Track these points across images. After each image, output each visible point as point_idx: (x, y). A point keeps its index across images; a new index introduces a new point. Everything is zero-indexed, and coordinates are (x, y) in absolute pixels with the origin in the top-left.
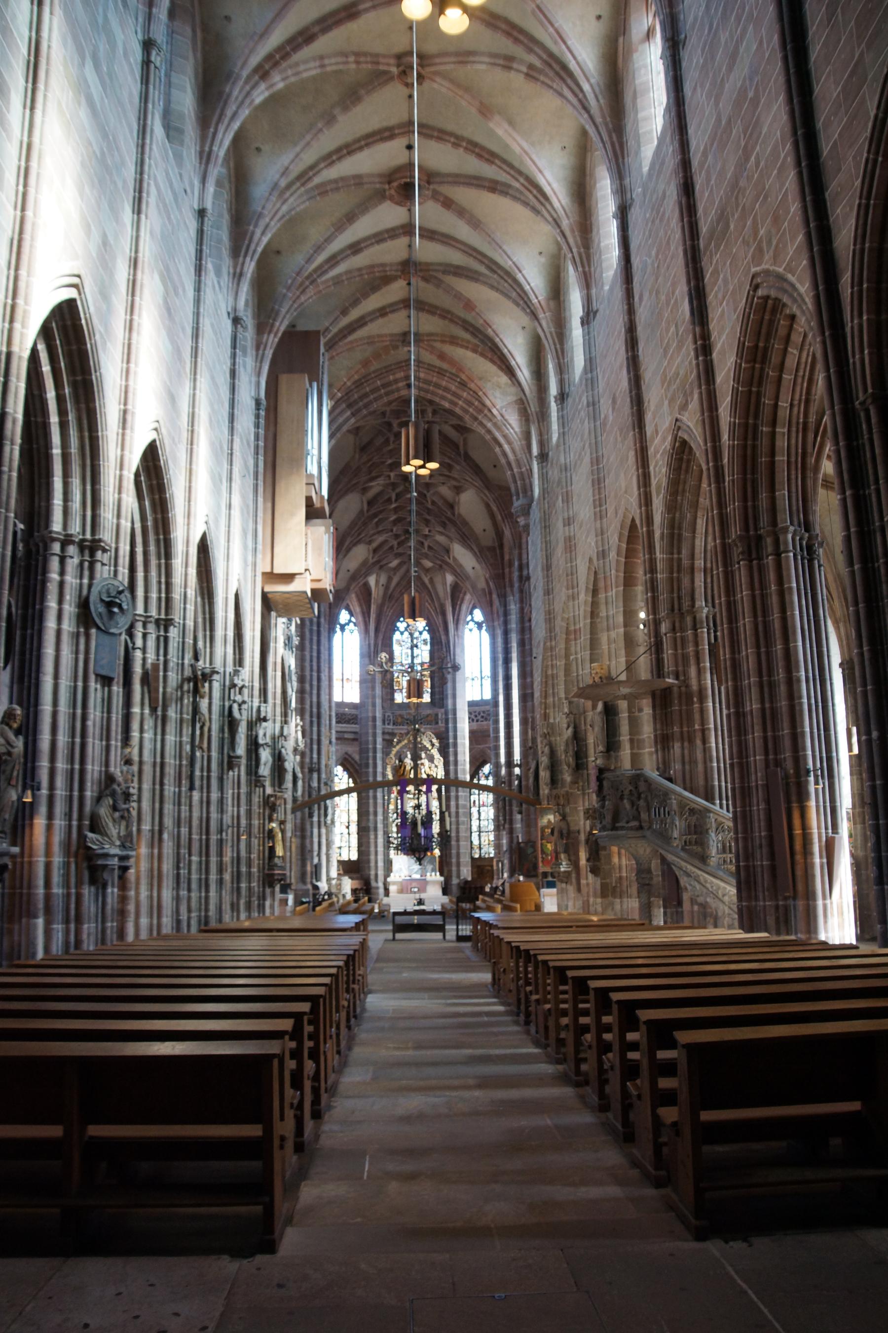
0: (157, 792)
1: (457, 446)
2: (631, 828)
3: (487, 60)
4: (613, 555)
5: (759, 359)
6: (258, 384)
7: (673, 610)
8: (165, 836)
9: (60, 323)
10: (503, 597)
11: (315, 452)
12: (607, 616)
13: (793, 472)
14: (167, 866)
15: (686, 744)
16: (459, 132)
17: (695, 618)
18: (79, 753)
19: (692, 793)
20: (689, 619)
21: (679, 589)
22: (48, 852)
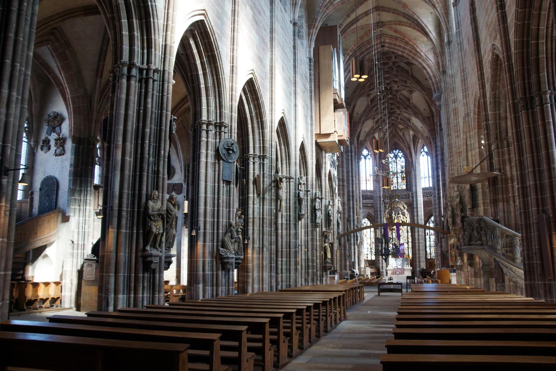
0: (261, 231)
2: (478, 245)
5: (527, 6)
7: (497, 138)
8: (265, 249)
9: (199, 31)
12: (471, 144)
13: (550, 62)
14: (266, 262)
15: (505, 203)
17: (508, 142)
18: (216, 214)
19: (509, 228)
20: (505, 142)
21: (500, 128)
22: (204, 257)
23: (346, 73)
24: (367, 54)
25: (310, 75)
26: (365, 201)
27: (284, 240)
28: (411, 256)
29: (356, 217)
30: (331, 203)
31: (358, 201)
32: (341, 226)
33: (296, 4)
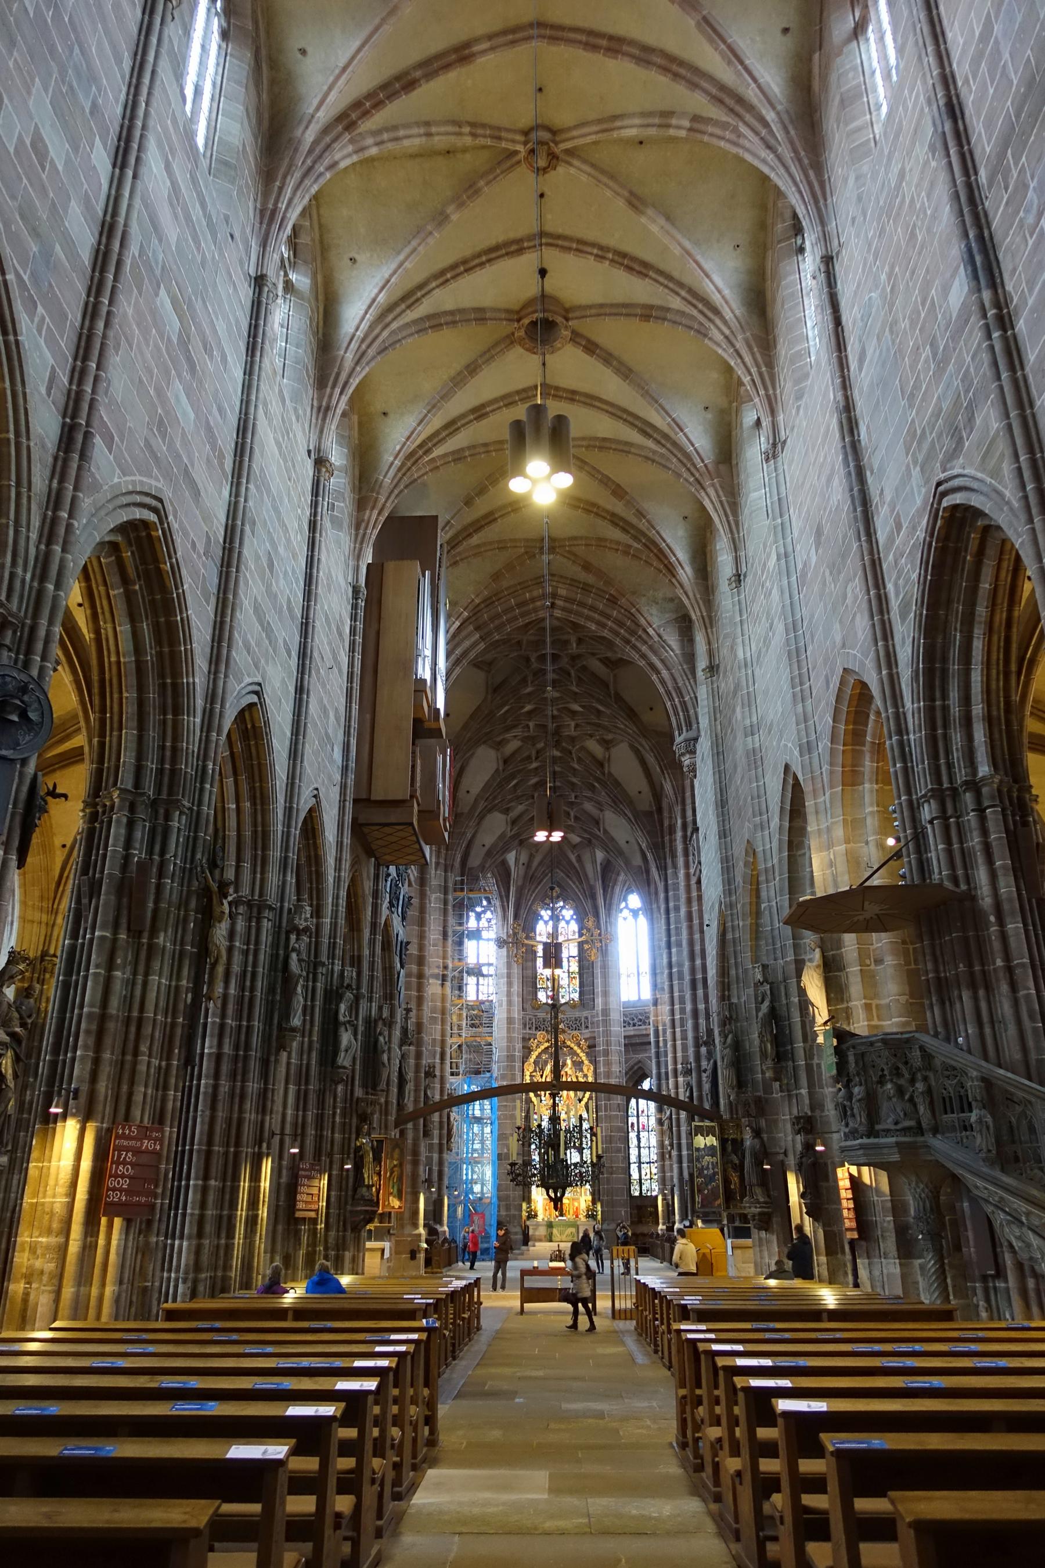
0: (128, 1067)
1: (607, 686)
3: (637, 121)
4: (824, 744)
10: (662, 868)
11: (428, 652)
16: (605, 241)
19: (1013, 1073)
23: (449, 664)
24: (509, 621)
25: (353, 631)
30: (385, 1014)
32: (410, 1087)
33: (328, 408)
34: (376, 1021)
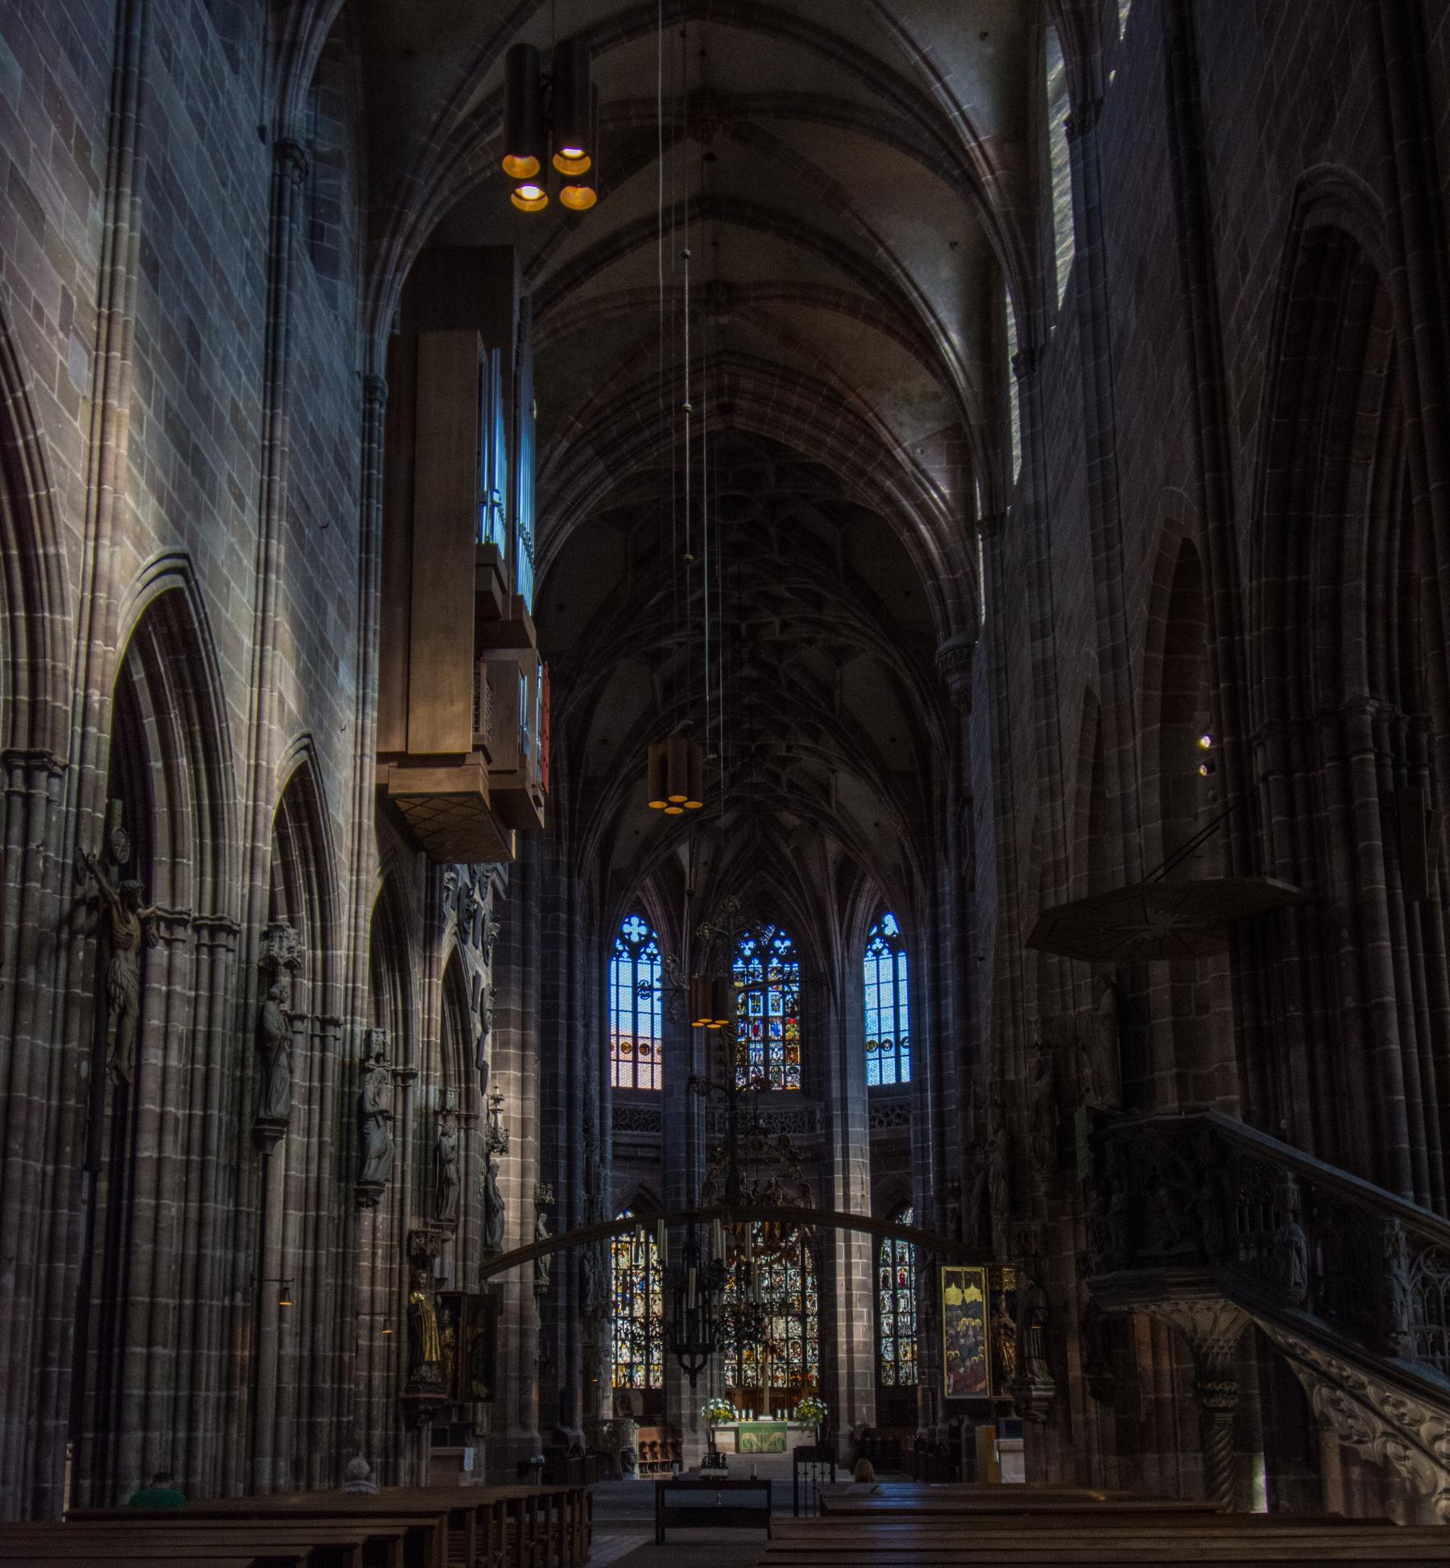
4: (1136, 653)
6: (370, 347)
26: (626, 1136)
27: (170, 1249)
28: (814, 1373)
29: (581, 1194)
31: (597, 1131)
34: (436, 1113)
